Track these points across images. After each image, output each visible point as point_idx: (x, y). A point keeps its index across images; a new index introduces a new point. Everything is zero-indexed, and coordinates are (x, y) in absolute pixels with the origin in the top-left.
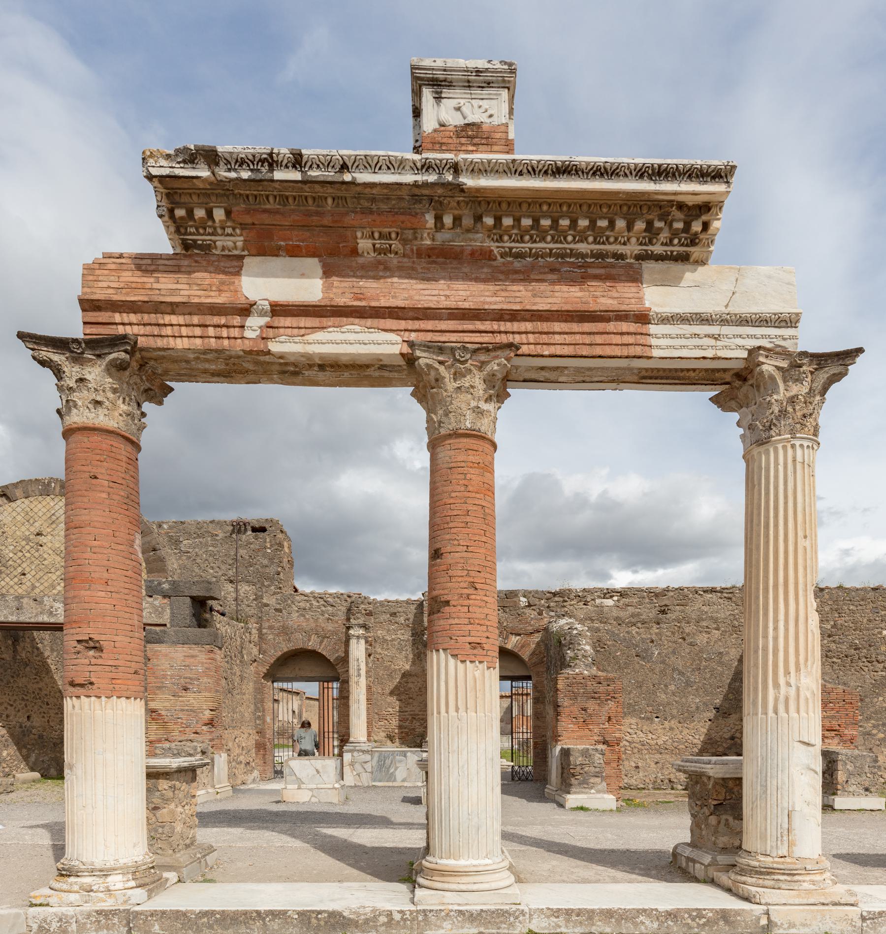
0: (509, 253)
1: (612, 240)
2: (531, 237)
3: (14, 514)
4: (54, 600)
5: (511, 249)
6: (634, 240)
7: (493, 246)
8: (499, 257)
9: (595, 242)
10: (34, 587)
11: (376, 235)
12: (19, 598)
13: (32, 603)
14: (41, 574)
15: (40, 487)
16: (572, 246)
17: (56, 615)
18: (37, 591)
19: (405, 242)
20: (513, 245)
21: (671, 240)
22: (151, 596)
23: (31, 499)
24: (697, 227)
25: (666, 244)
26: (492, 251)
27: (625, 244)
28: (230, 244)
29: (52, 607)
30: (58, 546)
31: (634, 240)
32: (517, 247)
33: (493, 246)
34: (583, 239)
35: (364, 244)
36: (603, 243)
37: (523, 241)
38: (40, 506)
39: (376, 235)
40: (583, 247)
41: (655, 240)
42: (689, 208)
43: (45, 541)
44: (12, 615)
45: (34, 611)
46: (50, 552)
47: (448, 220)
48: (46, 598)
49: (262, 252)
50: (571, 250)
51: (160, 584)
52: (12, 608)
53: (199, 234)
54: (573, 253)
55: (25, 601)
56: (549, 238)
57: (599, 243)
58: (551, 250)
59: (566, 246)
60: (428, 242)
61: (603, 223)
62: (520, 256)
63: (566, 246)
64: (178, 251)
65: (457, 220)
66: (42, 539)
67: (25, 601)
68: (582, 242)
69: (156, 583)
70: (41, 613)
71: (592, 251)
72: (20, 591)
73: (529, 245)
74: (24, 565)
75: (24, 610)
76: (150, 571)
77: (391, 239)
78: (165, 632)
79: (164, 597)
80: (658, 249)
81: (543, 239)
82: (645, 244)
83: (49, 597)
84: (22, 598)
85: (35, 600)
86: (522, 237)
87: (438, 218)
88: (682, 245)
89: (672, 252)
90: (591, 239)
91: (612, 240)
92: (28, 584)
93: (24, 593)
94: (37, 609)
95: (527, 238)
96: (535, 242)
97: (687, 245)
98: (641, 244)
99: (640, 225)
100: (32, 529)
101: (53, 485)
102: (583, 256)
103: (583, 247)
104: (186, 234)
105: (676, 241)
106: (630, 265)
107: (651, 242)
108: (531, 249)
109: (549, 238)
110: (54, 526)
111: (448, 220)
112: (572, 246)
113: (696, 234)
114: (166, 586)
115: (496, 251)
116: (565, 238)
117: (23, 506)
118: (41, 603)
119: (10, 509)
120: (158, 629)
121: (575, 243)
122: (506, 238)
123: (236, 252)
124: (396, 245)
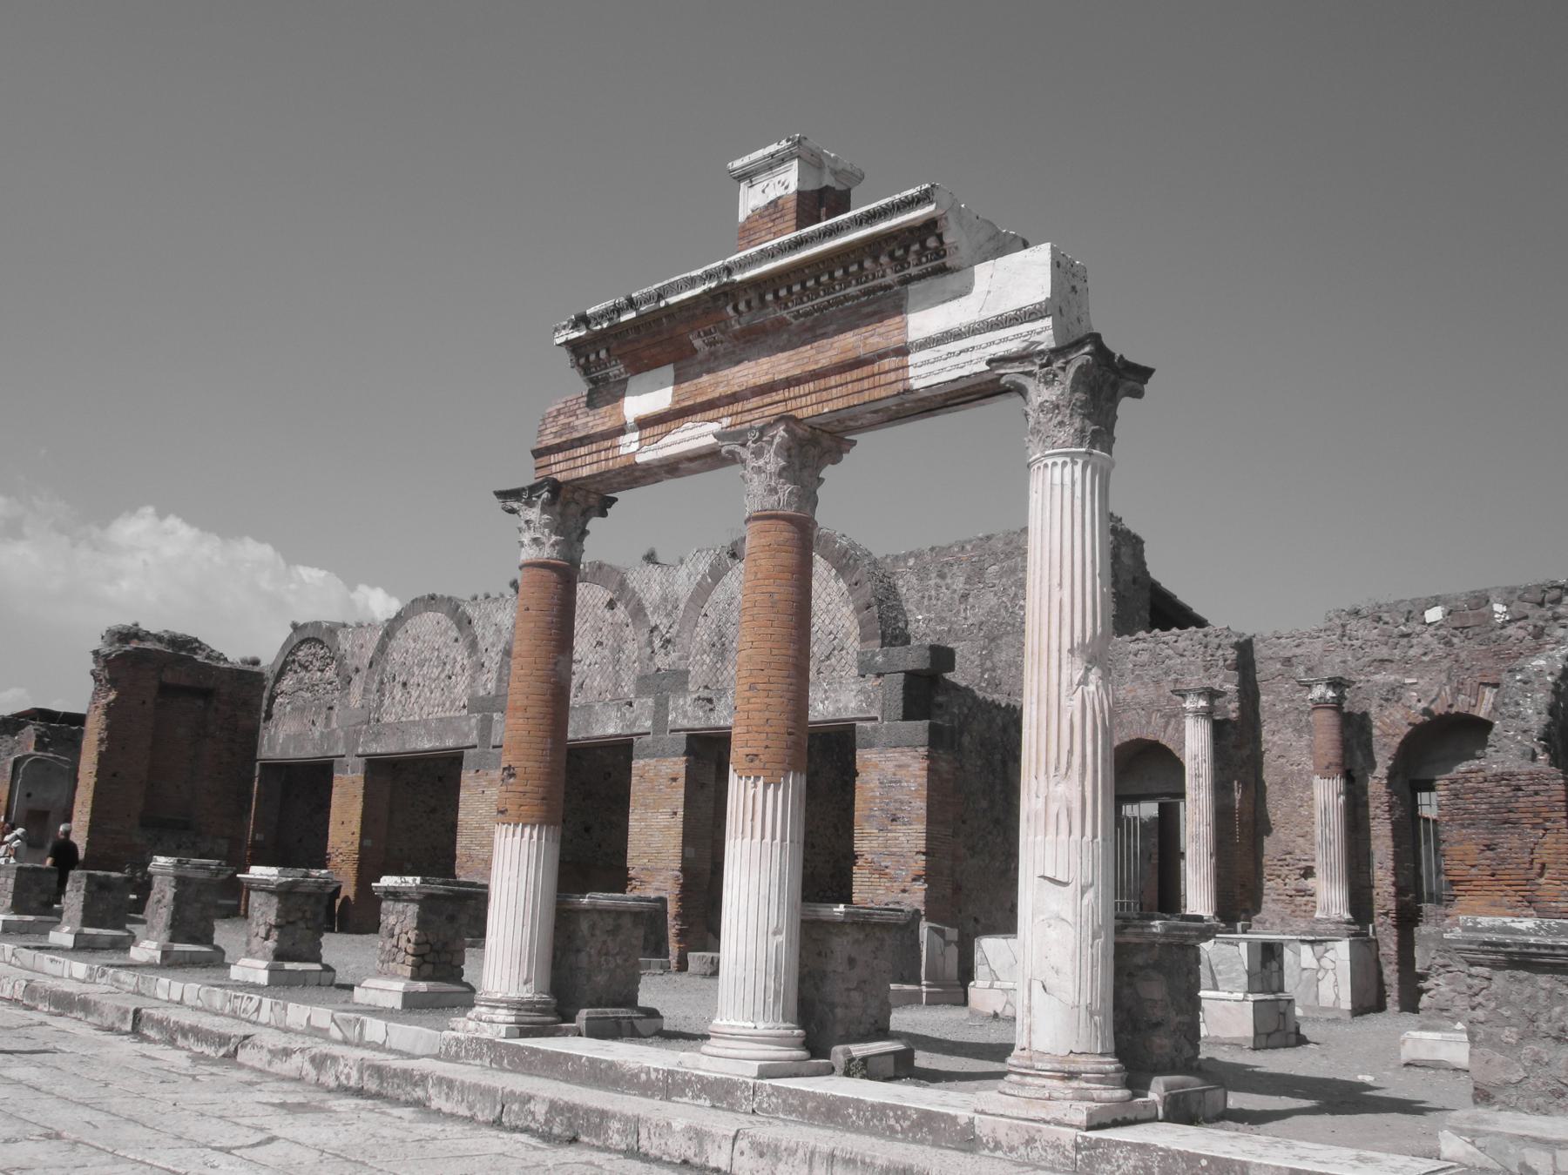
0: (797, 316)
1: (870, 277)
2: (808, 296)
5: (798, 311)
6: (888, 271)
7: (784, 313)
8: (793, 320)
9: (858, 283)
11: (702, 334)
16: (843, 293)
19: (723, 333)
20: (798, 307)
21: (920, 260)
22: (863, 676)
24: (932, 242)
25: (917, 265)
26: (785, 318)
27: (883, 276)
28: (617, 372)
31: (888, 271)
32: (803, 308)
33: (784, 313)
34: (848, 285)
35: (698, 343)
36: (866, 282)
37: (803, 303)
39: (702, 334)
40: (852, 290)
41: (906, 266)
42: (919, 228)
47: (742, 307)
49: (638, 371)
50: (844, 296)
53: (597, 371)
54: (847, 298)
56: (822, 293)
57: (862, 283)
58: (828, 301)
59: (838, 294)
60: (738, 327)
61: (854, 268)
62: (807, 314)
63: (838, 294)
64: (591, 386)
65: (748, 303)
68: (849, 286)
71: (860, 291)
73: (810, 303)
77: (711, 333)
79: (879, 675)
80: (913, 271)
81: (818, 296)
82: (900, 271)
86: (801, 299)
87: (735, 309)
88: (931, 260)
89: (927, 269)
90: (854, 282)
91: (870, 277)
95: (805, 299)
96: (812, 300)
97: (936, 259)
98: (896, 272)
99: (884, 259)
102: (857, 297)
103: (852, 290)
104: (591, 373)
105: (924, 260)
106: (897, 293)
107: (903, 269)
108: (813, 306)
109: (822, 293)
111: (742, 307)
112: (843, 293)
113: (936, 248)
115: (788, 317)
116: (834, 289)
121: (845, 288)
122: (790, 304)
123: (623, 376)
124: (718, 336)
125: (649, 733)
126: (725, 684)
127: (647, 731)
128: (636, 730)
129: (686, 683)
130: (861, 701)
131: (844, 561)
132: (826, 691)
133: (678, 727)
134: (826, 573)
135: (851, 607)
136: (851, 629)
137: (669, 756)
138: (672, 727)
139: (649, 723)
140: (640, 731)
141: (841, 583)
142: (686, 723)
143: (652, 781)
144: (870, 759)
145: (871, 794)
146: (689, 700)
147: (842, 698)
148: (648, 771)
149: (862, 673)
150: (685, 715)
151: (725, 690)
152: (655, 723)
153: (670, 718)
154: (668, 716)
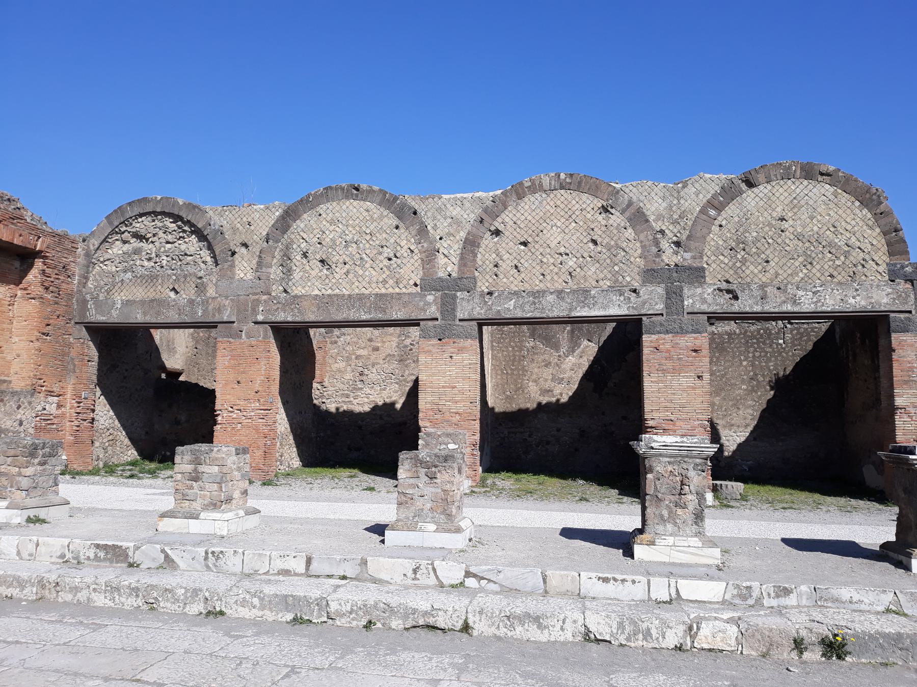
3: (757, 199)
4: (798, 288)
10: (777, 275)
12: (763, 287)
13: (776, 291)
14: (784, 260)
15: (781, 171)
17: (799, 304)
18: (780, 278)
23: (774, 183)
29: (795, 296)
30: (800, 231)
38: (781, 190)
43: (786, 226)
44: (757, 304)
45: (778, 300)
46: (792, 237)
48: (790, 286)
51: (903, 267)
52: (756, 297)
55: (769, 289)
66: (785, 225)
67: (769, 289)
69: (899, 266)
70: (785, 302)
72: (764, 279)
74: (768, 252)
75: (768, 300)
76: (891, 254)
78: (909, 319)
83: (792, 285)
84: (766, 287)
85: (779, 288)
92: (772, 271)
93: (768, 281)
94: (780, 298)
100: (774, 214)
101: (794, 168)
110: (795, 210)
114: (909, 269)
117: (766, 191)
118: (785, 291)
119: (753, 195)
120: (902, 316)
125: (662, 315)
126: (749, 280)
127: (659, 312)
128: (643, 312)
129: (704, 277)
130: (894, 299)
131: (868, 196)
132: (857, 290)
133: (696, 311)
134: (849, 204)
135: (878, 230)
136: (879, 246)
137: (687, 332)
138: (690, 310)
139: (660, 307)
140: (649, 312)
141: (865, 211)
142: (705, 308)
143: (668, 351)
144: (905, 341)
145: (909, 365)
146: (710, 291)
147: (874, 296)
148: (663, 344)
149: (893, 279)
150: (704, 301)
151: (748, 284)
152: (667, 307)
153: (686, 303)
154: (683, 301)
